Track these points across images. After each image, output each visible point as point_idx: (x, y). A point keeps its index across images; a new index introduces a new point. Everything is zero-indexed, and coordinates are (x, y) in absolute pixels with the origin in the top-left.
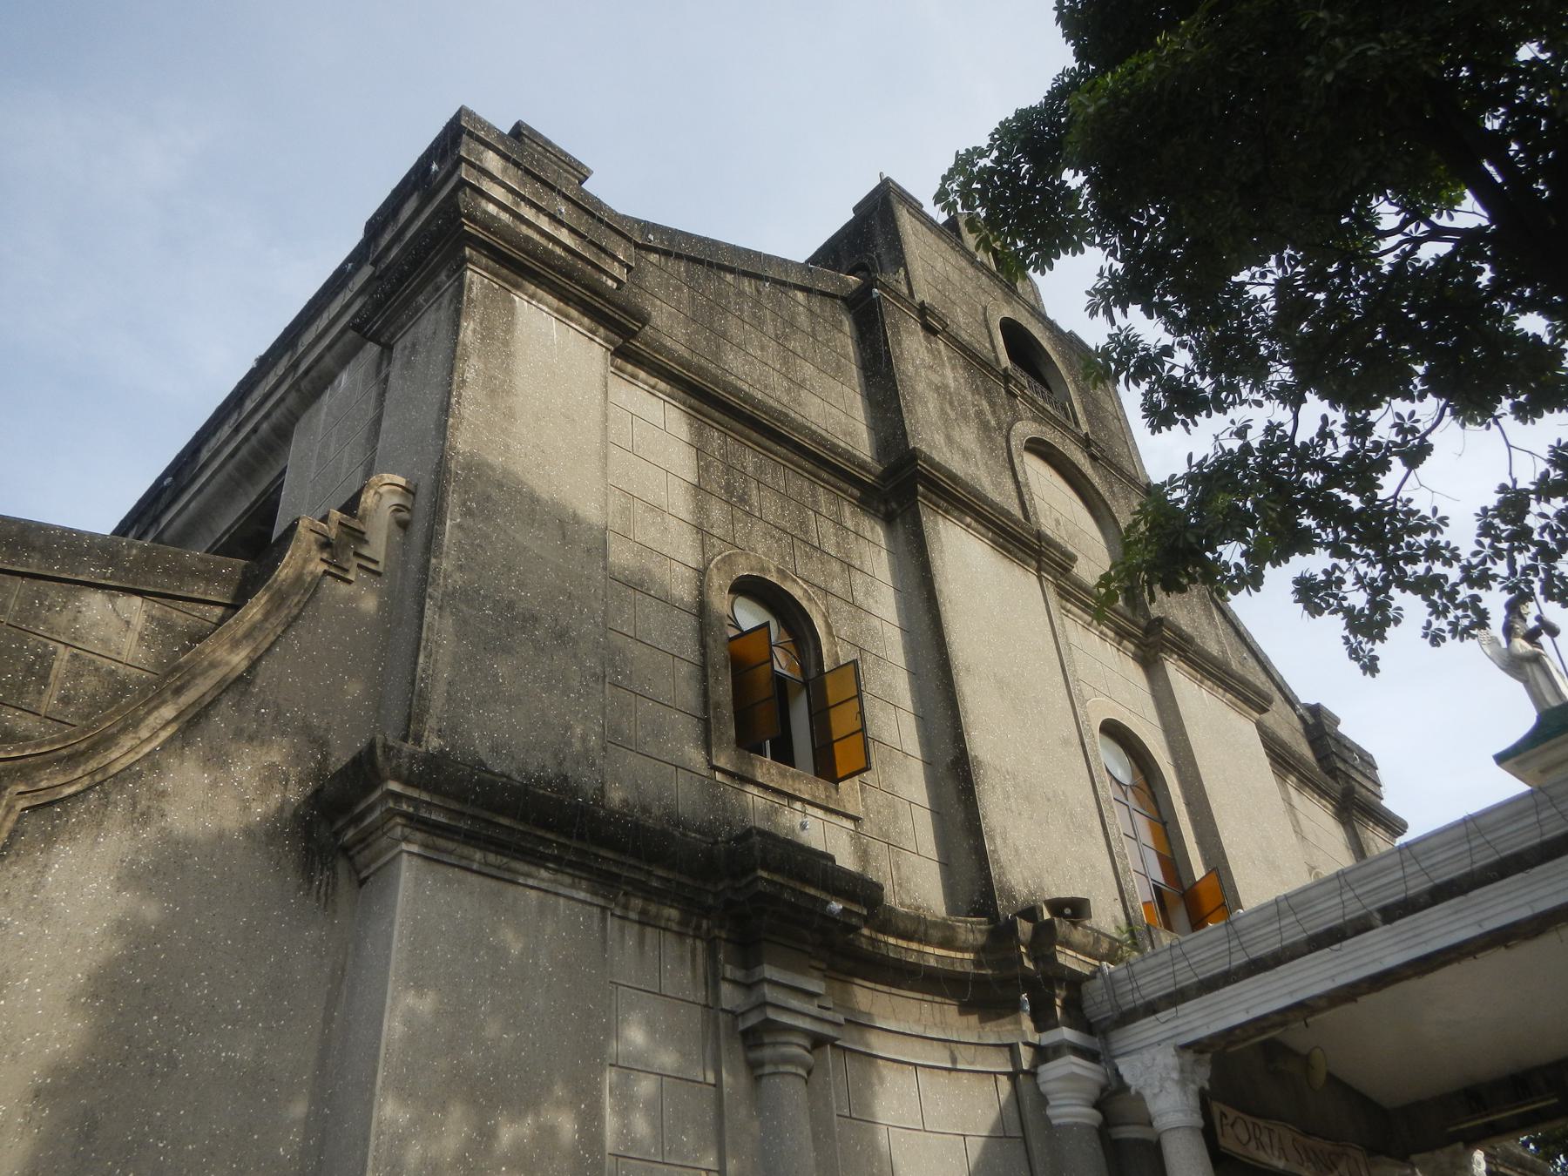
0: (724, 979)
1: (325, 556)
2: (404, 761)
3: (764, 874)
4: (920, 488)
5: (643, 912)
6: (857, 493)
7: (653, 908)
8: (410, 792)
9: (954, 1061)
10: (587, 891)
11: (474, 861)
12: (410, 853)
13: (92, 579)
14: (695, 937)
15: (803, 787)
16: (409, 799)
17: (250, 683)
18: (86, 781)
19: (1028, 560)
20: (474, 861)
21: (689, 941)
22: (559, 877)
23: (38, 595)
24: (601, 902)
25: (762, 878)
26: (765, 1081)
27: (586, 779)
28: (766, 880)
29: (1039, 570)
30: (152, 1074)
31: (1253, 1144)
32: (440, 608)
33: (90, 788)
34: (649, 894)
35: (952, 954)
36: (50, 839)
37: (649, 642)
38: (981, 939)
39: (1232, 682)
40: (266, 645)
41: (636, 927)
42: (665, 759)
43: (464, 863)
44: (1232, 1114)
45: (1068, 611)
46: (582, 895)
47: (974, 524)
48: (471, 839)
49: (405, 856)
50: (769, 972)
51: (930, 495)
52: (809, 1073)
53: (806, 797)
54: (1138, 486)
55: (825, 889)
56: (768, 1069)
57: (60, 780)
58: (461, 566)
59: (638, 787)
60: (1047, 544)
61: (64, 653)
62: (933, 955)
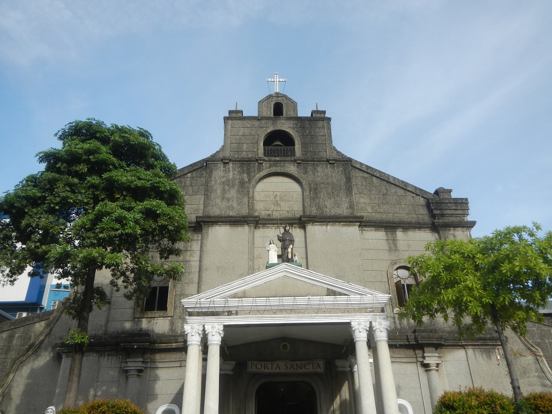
1: (63, 306)
2: (58, 345)
3: (122, 344)
4: (202, 224)
6: (192, 229)
7: (110, 353)
9: (181, 364)
14: (120, 355)
15: (157, 314)
16: (62, 350)
17: (51, 333)
18: (26, 357)
19: (243, 224)
21: (119, 356)
23: (29, 327)
24: (99, 355)
26: (129, 379)
27: (100, 332)
29: (248, 225)
31: (263, 369)
33: (27, 358)
34: (108, 351)
35: (179, 344)
36: (23, 367)
38: (183, 340)
39: (340, 220)
41: (107, 357)
42: (124, 320)
44: (255, 363)
45: (268, 227)
47: (221, 224)
50: (128, 360)
51: (205, 224)
52: (138, 375)
53: (157, 316)
54: (323, 161)
55: (135, 343)
56: (128, 377)
60: (245, 217)
61: (33, 334)
62: (174, 345)
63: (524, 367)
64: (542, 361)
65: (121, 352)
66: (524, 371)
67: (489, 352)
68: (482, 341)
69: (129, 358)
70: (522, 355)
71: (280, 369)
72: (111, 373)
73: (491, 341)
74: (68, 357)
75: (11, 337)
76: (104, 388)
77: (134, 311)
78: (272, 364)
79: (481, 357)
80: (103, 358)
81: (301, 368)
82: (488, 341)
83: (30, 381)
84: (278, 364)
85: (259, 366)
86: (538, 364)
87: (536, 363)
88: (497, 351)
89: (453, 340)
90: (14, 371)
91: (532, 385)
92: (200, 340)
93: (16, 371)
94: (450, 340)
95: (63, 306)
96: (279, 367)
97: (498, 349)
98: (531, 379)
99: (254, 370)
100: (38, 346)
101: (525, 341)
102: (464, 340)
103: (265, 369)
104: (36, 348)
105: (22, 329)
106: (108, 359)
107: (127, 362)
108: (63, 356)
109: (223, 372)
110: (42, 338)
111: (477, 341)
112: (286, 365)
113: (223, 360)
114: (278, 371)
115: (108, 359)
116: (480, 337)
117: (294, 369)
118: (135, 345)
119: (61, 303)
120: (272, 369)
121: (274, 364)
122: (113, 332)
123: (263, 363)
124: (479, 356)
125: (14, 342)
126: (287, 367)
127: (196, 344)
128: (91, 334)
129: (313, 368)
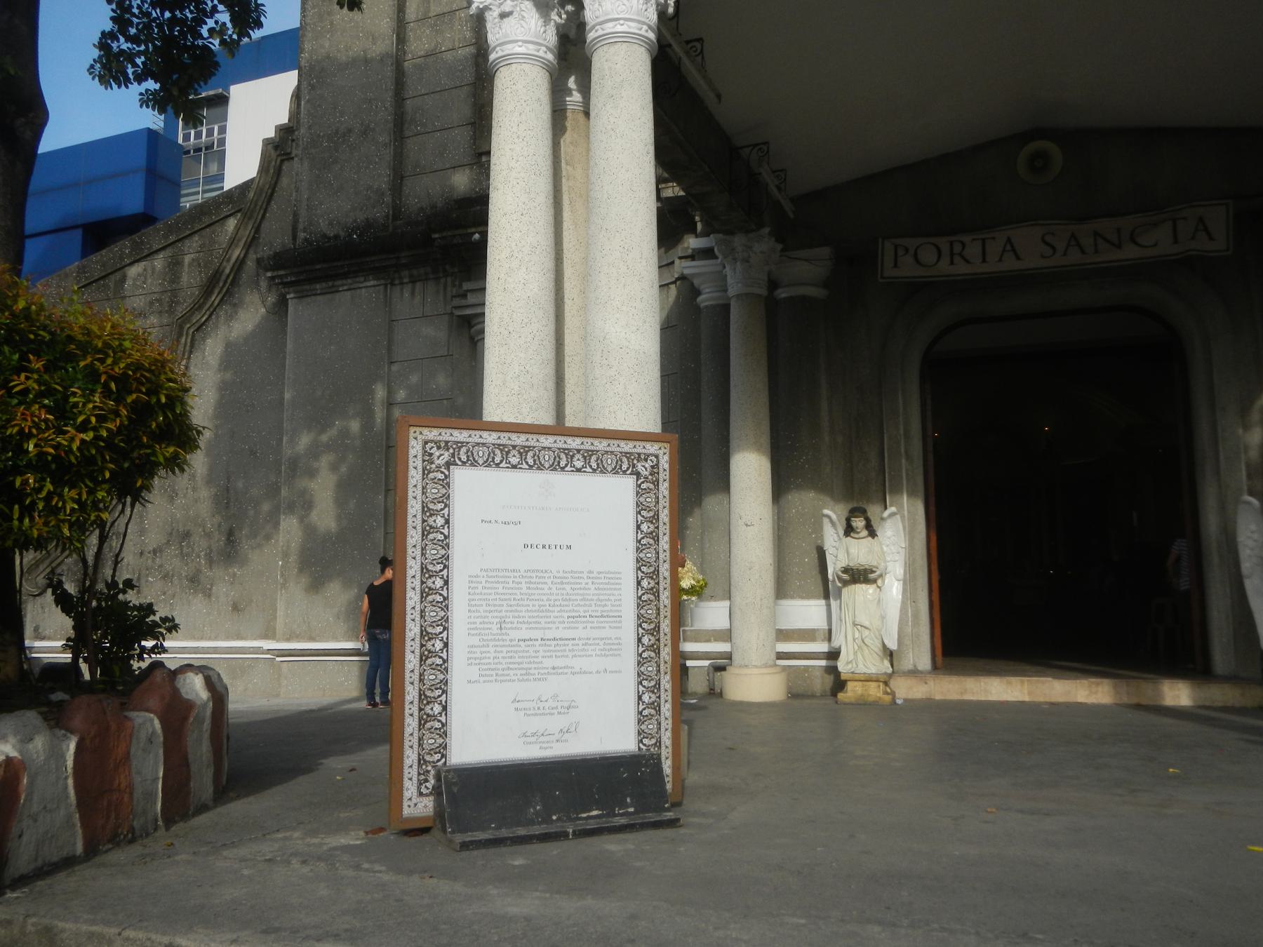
0: (455, 297)
3: (436, 236)
5: (411, 276)
7: (415, 272)
8: (275, 274)
10: (374, 279)
11: (317, 290)
12: (291, 298)
13: (226, 214)
16: (280, 277)
17: (259, 238)
18: (208, 313)
20: (317, 290)
21: (443, 280)
22: (357, 279)
24: (383, 282)
25: (436, 238)
27: (379, 213)
28: (439, 238)
30: (248, 411)
32: (301, 159)
33: (210, 316)
36: (204, 340)
37: (439, 89)
40: (260, 217)
41: (410, 285)
43: (314, 292)
46: (372, 283)
48: (311, 281)
49: (290, 300)
56: (476, 339)
57: (199, 316)
58: (310, 126)
59: (429, 194)
65: (447, 267)
69: (469, 280)
71: (1018, 258)
72: (428, 331)
74: (303, 297)
75: (175, 265)
76: (414, 379)
77: (474, 132)
78: (984, 240)
80: (398, 288)
81: (1119, 246)
83: (228, 376)
84: (1009, 240)
85: (928, 256)
90: (184, 355)
92: (551, 38)
93: (191, 352)
95: (278, 152)
96: (1014, 250)
99: (908, 270)
100: (231, 278)
103: (952, 263)
104: (227, 285)
105: (195, 242)
106: (413, 293)
107: (464, 296)
108: (288, 297)
109: (782, 293)
110: (237, 253)
112: (1048, 238)
113: (780, 247)
114: (1010, 264)
115: (413, 293)
117: (1083, 252)
118: (475, 233)
119: (270, 147)
120: (984, 261)
121: (994, 238)
122: (422, 209)
123: (943, 242)
125: (185, 278)
126: (1053, 248)
127: (527, 57)
128: (355, 221)
129: (1176, 241)
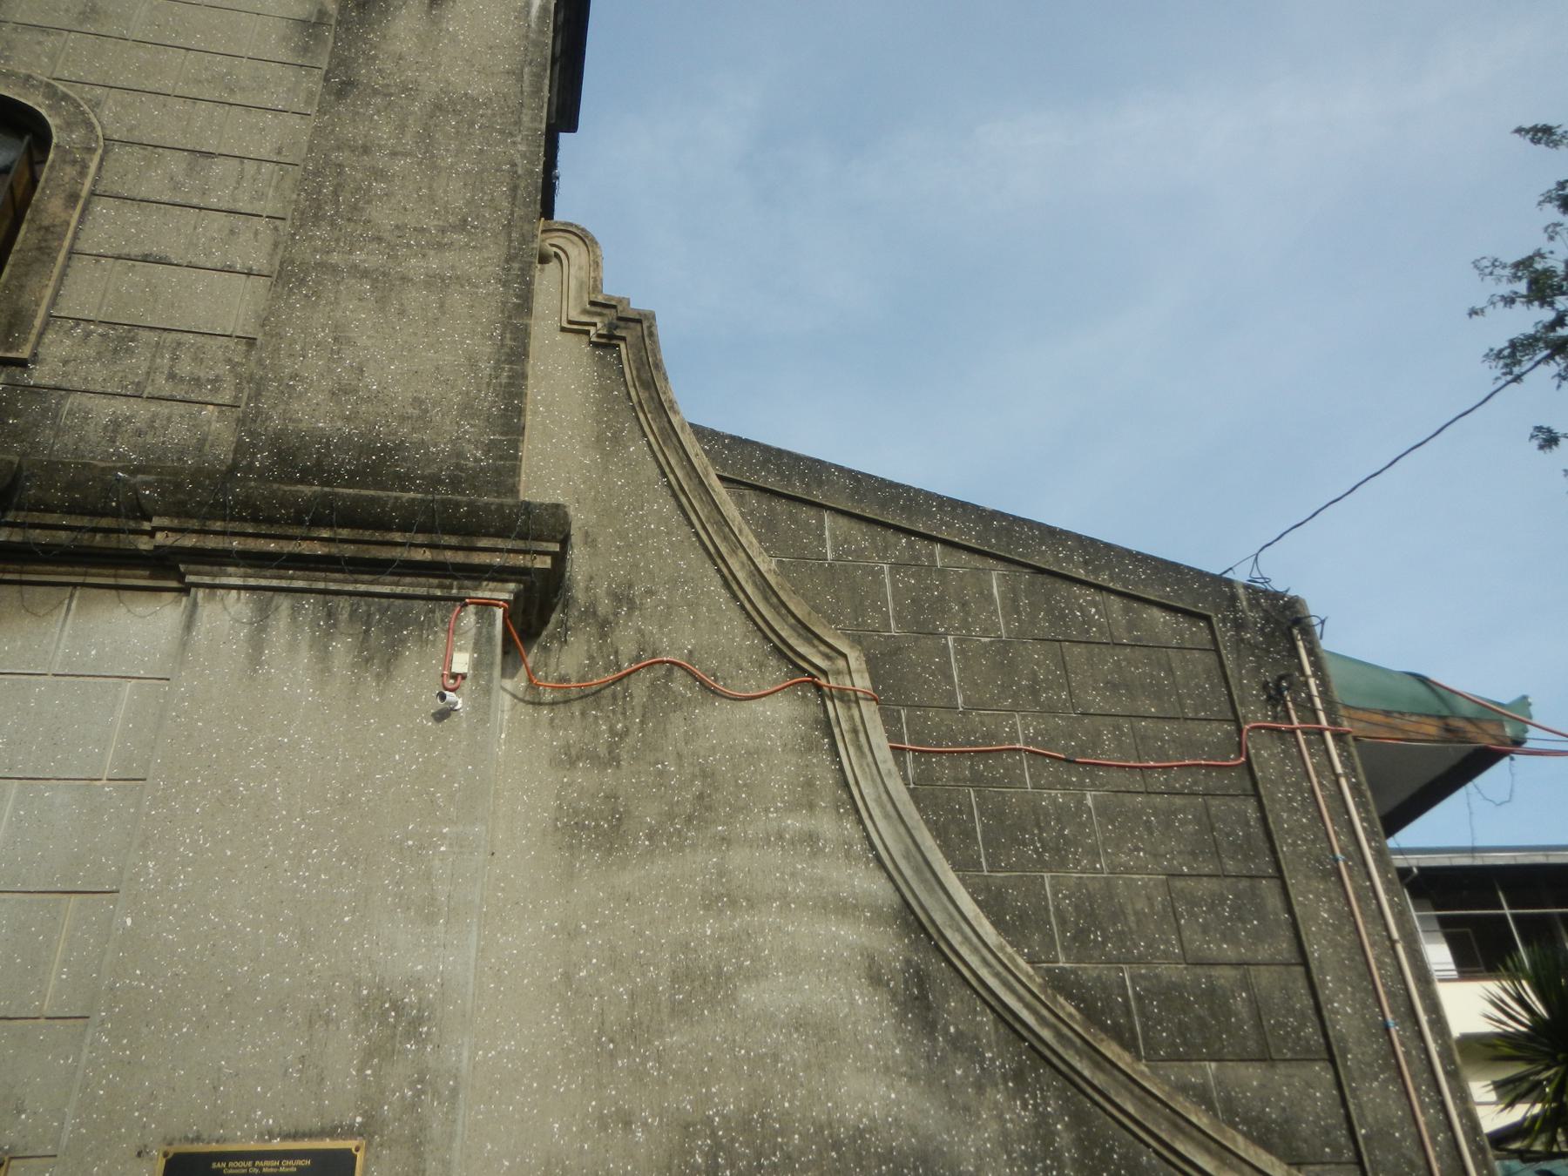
63: (706, 774)
64: (855, 731)
66: (701, 797)
67: (401, 621)
68: (344, 533)
70: (715, 692)
73: (420, 538)
79: (305, 656)
82: (397, 537)
86: (827, 758)
87: (811, 747)
88: (469, 618)
89: (73, 509)
91: (733, 903)
94: (50, 509)
97: (485, 606)
98: (738, 858)
101: (766, 599)
102: (180, 510)
111: (297, 531)
116: (326, 501)
124: (293, 647)
